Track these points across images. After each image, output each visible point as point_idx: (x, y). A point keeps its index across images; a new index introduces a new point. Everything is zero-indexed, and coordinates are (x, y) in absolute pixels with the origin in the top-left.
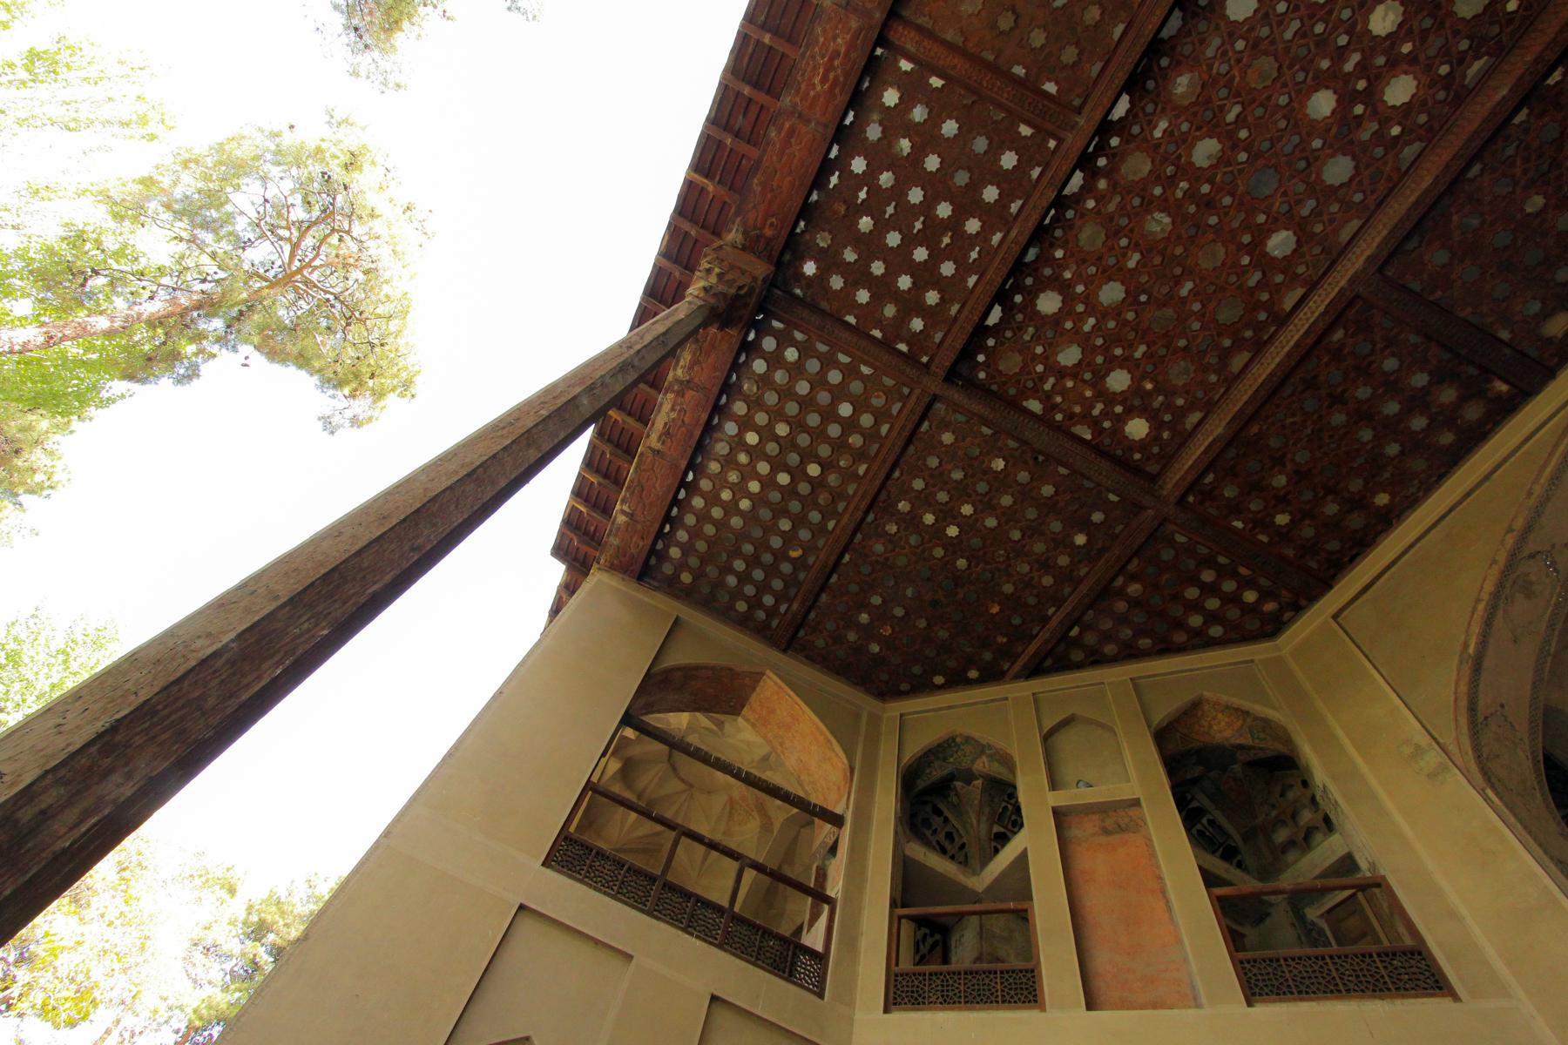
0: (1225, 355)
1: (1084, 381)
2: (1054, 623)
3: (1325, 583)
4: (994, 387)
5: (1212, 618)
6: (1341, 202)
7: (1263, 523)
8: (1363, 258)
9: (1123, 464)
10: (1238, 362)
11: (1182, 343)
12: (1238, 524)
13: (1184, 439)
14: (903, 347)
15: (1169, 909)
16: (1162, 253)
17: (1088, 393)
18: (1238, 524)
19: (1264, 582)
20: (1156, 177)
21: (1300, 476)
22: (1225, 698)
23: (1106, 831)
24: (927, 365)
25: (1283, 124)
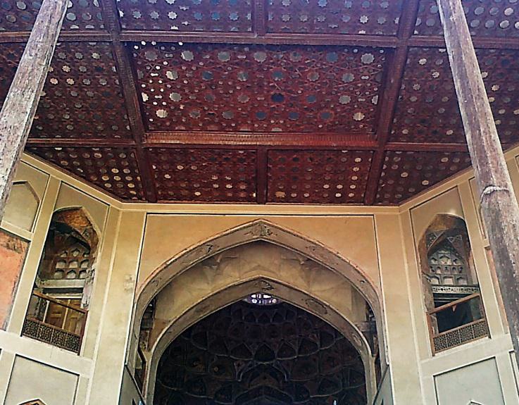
0: (212, 122)
1: (166, 86)
2: (54, 141)
3: (155, 199)
4: (135, 55)
5: (112, 181)
6: (285, 122)
7: (161, 173)
8: (269, 143)
9: (145, 119)
10: (213, 127)
11: (206, 108)
12: (154, 167)
13: (171, 129)
14: (121, 14)
15: (14, 290)
16: (234, 83)
17: (162, 90)
18: (154, 167)
19: (140, 186)
20: (260, 66)
21: (187, 171)
22: (88, 214)
23: (8, 246)
24: (122, 29)
25: (300, 92)
